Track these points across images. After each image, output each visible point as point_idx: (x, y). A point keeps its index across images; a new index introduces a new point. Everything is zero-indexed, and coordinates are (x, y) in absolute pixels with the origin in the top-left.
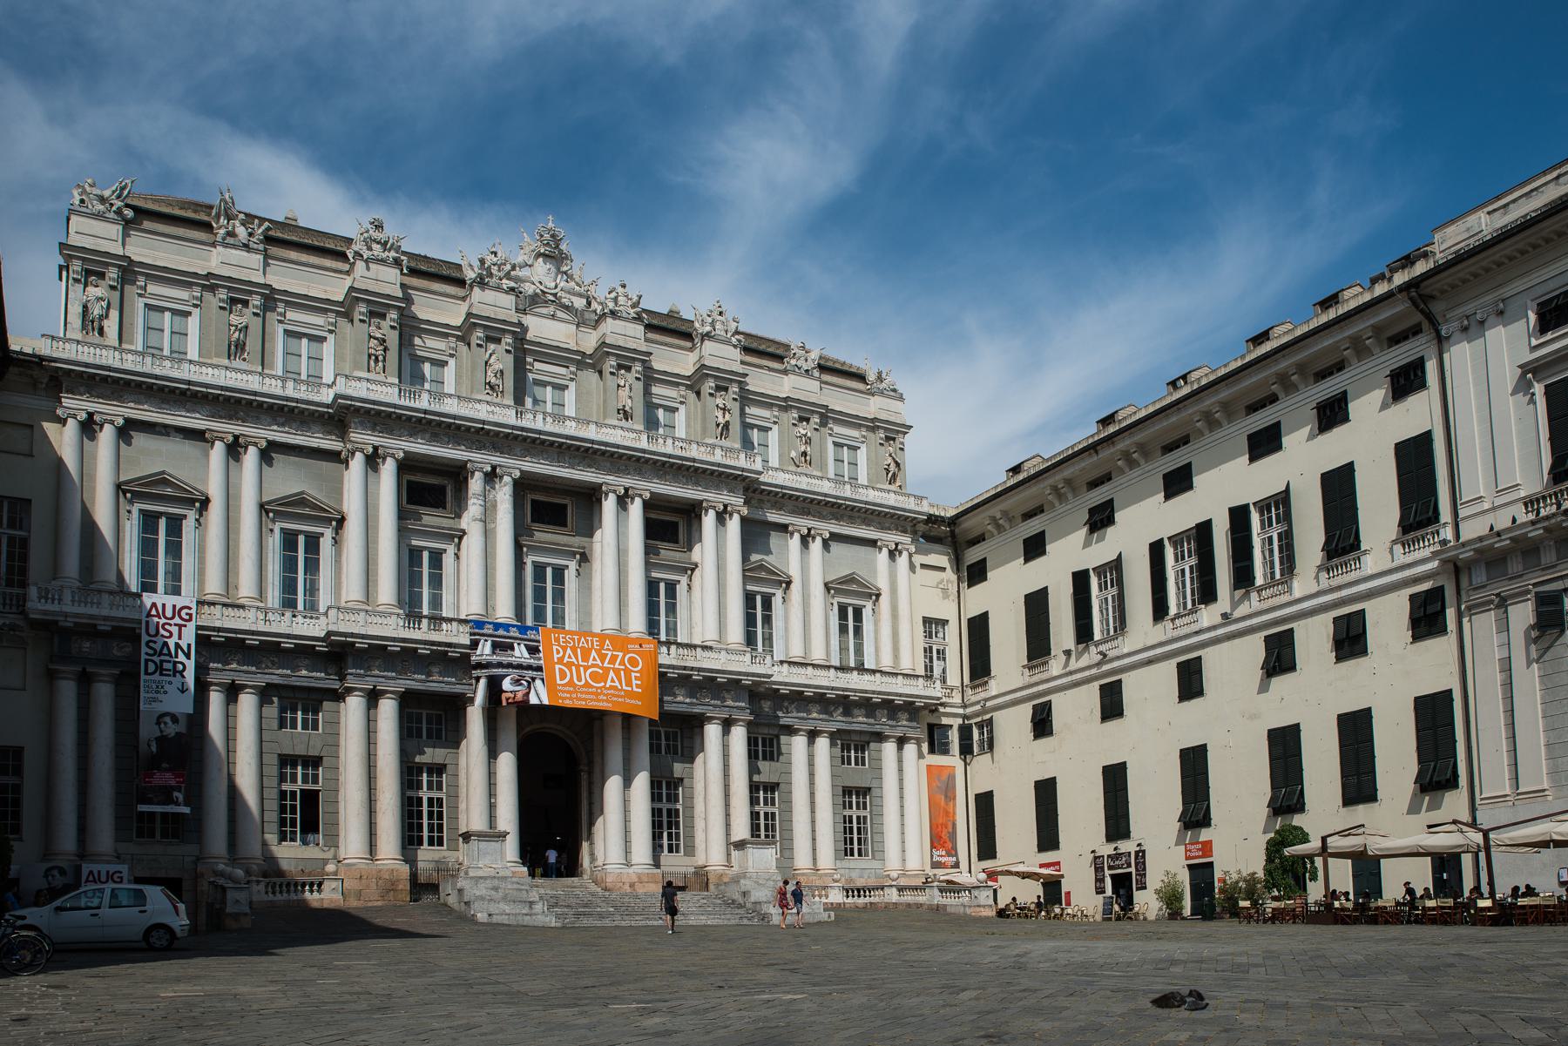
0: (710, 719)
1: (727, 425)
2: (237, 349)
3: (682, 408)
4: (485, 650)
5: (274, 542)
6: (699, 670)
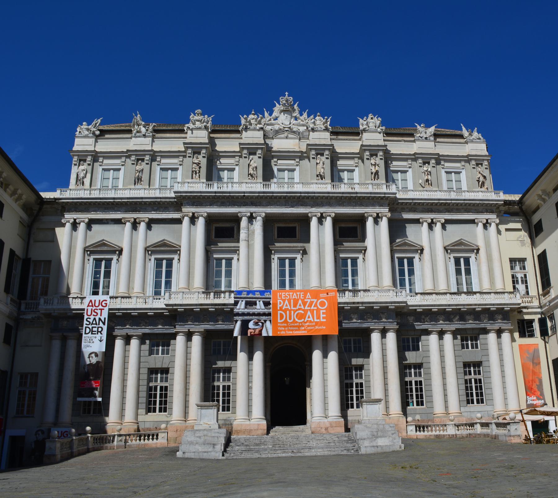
0: (372, 331)
1: (377, 173)
2: (138, 180)
3: (357, 169)
4: (241, 307)
5: (151, 265)
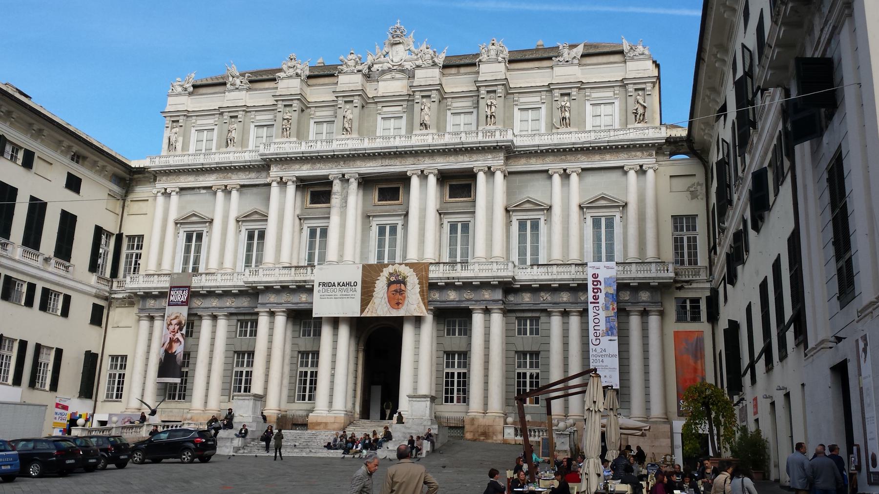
6: (458, 278)
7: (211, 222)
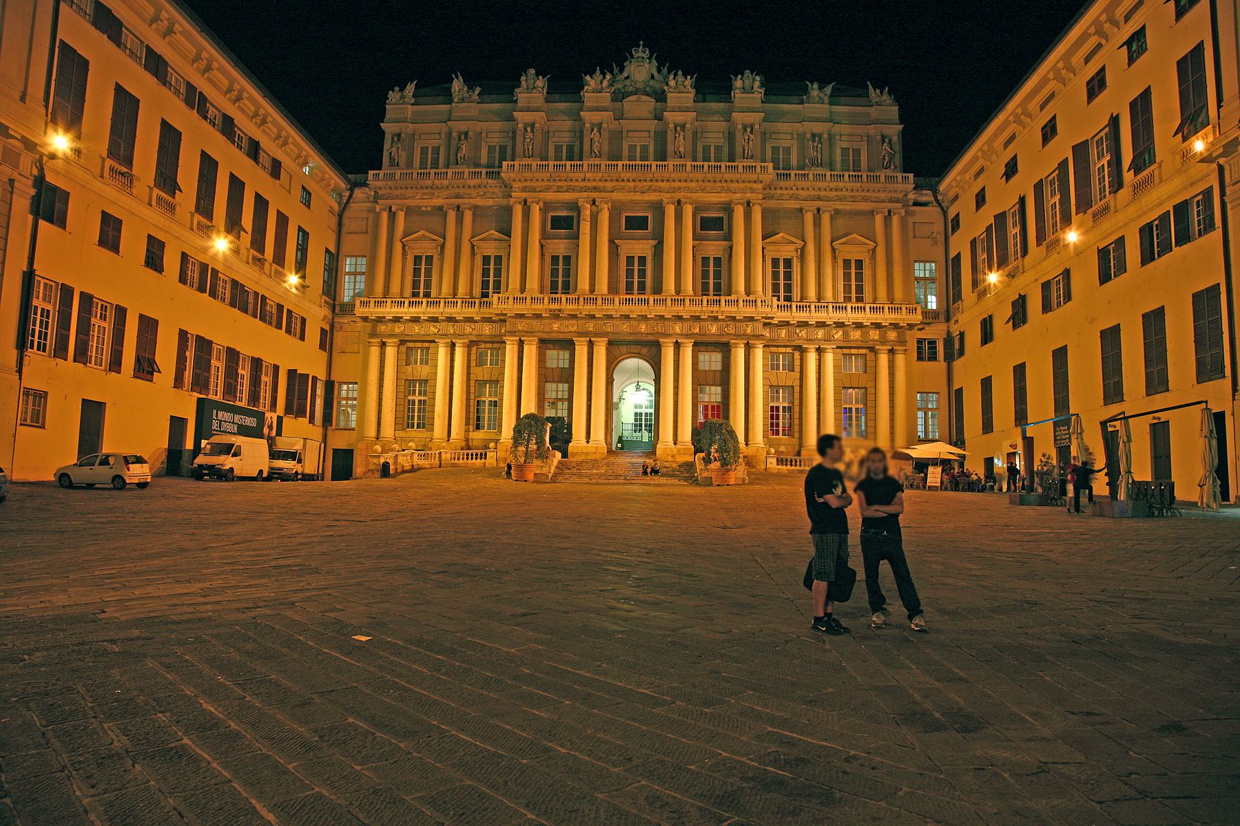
7: (443, 246)
